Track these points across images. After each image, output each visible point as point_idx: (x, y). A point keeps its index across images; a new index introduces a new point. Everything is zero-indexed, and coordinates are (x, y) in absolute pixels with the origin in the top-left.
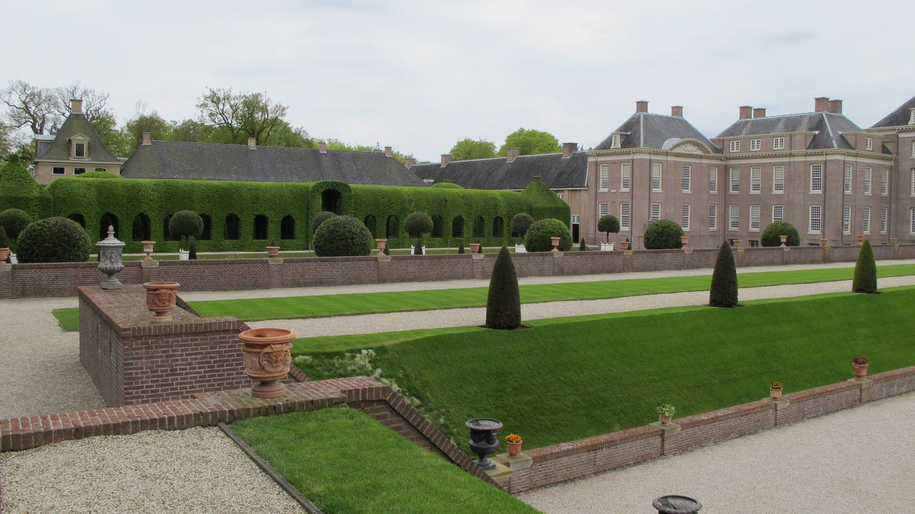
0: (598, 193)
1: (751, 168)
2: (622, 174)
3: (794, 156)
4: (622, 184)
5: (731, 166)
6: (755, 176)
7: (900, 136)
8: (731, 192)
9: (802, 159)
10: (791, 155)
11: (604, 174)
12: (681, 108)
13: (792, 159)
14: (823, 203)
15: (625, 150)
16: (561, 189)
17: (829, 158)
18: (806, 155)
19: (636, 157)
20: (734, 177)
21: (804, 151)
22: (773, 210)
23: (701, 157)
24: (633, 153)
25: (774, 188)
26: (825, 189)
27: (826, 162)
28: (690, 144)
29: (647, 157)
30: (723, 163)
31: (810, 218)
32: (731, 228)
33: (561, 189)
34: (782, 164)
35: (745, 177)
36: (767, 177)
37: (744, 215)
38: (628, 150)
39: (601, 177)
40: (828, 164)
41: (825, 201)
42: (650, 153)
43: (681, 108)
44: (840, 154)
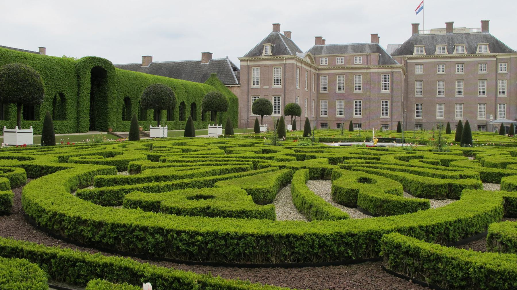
0: (250, 89)
1: (337, 76)
2: (273, 75)
3: (370, 68)
4: (273, 82)
5: (322, 74)
6: (340, 81)
7: (408, 61)
8: (321, 91)
9: (376, 71)
10: (368, 68)
11: (256, 74)
12: (290, 32)
13: (368, 71)
14: (391, 98)
15: (275, 57)
16: (231, 86)
17: (395, 70)
18: (378, 68)
19: (288, 62)
20: (324, 81)
21: (378, 66)
22: (354, 103)
23: (311, 66)
24: (286, 59)
30: (317, 72)
32: (321, 116)
33: (231, 86)
34: (361, 73)
35: (332, 81)
36: (349, 82)
37: (332, 107)
38: (278, 57)
39: (252, 76)
41: (392, 97)
43: (290, 32)
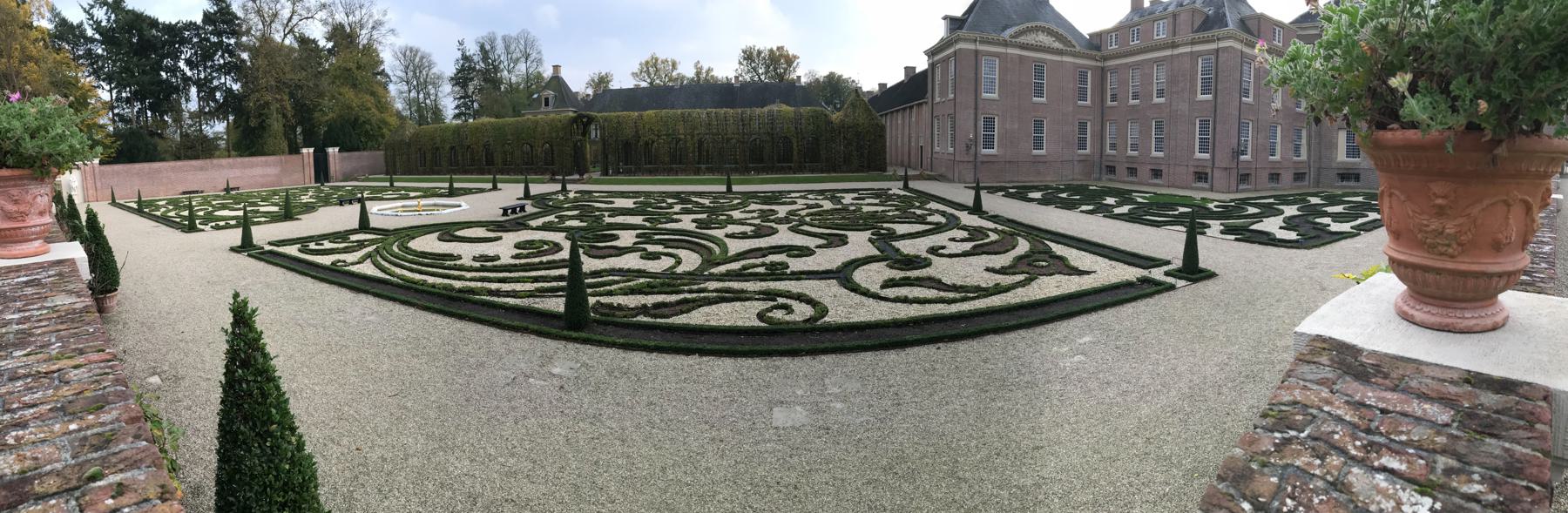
8: (1109, 103)
9: (1187, 49)
13: (1176, 52)
14: (1213, 115)
18: (1193, 43)
21: (1191, 36)
22: (1154, 127)
25: (1155, 95)
26: (1216, 93)
27: (1217, 50)
28: (1043, 32)
29: (971, 46)
30: (1099, 64)
31: (1197, 136)
34: (1164, 59)
40: (1220, 54)
41: (1215, 111)
42: (975, 41)
44: (1236, 39)
